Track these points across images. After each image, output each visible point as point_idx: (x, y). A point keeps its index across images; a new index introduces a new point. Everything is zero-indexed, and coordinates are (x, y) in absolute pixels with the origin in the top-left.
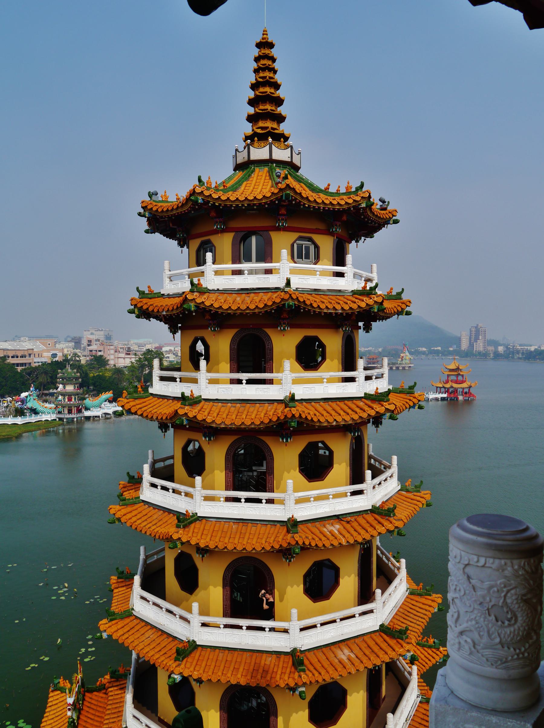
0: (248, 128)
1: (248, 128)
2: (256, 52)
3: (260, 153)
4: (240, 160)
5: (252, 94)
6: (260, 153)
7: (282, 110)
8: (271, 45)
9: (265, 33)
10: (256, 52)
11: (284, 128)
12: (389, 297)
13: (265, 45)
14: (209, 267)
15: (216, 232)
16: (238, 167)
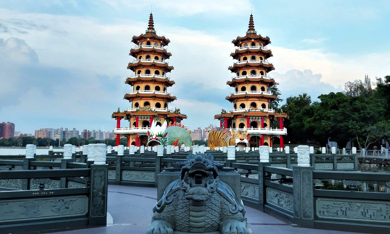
0: (148, 27)
1: (148, 27)
2: (150, 16)
3: (150, 31)
4: (147, 32)
5: (149, 22)
6: (150, 31)
7: (153, 25)
8: (152, 15)
9: (151, 13)
10: (150, 16)
11: (154, 27)
12: (169, 53)
13: (151, 15)
14: (143, 46)
15: (143, 41)
16: (146, 33)
